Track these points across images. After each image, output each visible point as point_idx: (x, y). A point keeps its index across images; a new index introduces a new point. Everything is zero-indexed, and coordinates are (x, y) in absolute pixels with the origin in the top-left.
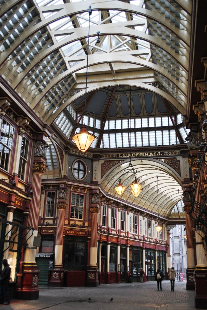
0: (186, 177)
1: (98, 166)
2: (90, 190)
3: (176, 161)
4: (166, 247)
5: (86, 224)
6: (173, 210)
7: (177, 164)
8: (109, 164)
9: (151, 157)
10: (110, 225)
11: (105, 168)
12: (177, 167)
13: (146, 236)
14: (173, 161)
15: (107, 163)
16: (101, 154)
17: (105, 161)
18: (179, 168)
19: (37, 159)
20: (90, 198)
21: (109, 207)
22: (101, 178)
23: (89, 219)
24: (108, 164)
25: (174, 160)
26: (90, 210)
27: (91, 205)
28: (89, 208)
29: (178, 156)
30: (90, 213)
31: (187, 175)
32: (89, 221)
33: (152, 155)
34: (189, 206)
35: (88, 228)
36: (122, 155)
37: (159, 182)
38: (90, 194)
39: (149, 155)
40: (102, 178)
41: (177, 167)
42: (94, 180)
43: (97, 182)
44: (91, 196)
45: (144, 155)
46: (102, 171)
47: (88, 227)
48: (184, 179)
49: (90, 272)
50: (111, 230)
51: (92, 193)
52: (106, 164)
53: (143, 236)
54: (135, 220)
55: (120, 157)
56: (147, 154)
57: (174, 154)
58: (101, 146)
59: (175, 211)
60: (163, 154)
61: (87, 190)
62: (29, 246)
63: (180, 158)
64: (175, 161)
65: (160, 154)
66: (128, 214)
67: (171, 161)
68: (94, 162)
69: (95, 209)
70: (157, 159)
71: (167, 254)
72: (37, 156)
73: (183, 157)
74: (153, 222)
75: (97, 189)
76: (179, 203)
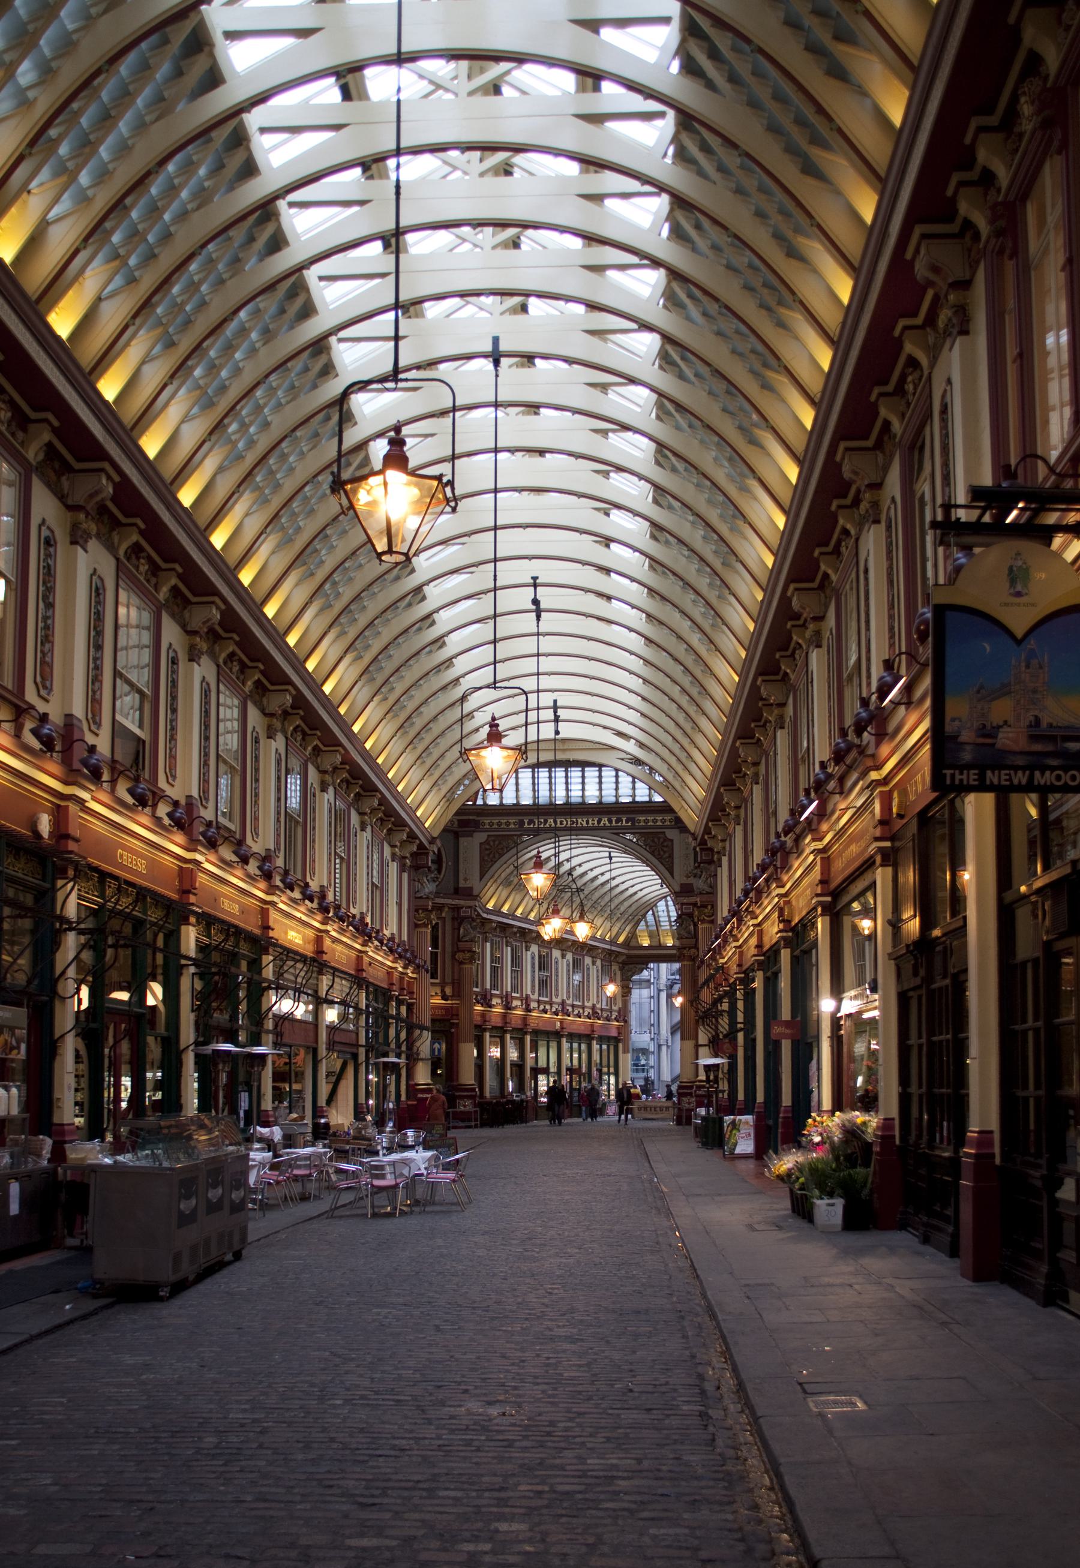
1: (471, 846)
2: (456, 909)
3: (665, 840)
4: (618, 1028)
5: (448, 991)
6: (643, 923)
9: (605, 828)
10: (488, 986)
12: (667, 855)
13: (569, 1002)
15: (494, 841)
18: (671, 856)
19: (421, 902)
20: (454, 929)
21: (486, 940)
23: (453, 979)
25: (659, 839)
29: (667, 827)
30: (456, 964)
32: (453, 983)
33: (608, 824)
36: (531, 822)
37: (614, 873)
38: (453, 919)
39: (599, 822)
42: (462, 884)
43: (471, 889)
45: (587, 822)
47: (453, 997)
48: (682, 885)
49: (462, 1097)
50: (492, 995)
51: (458, 918)
53: (563, 1003)
54: (544, 963)
55: (526, 826)
56: (593, 821)
57: (659, 823)
58: (480, 802)
59: (647, 926)
60: (633, 820)
61: (446, 909)
62: (422, 1056)
63: (671, 834)
65: (627, 822)
66: (527, 949)
67: (653, 841)
68: (461, 840)
69: (468, 955)
70: (618, 834)
71: (620, 1045)
72: (421, 898)
74: (588, 960)
75: (470, 907)
76: (661, 905)
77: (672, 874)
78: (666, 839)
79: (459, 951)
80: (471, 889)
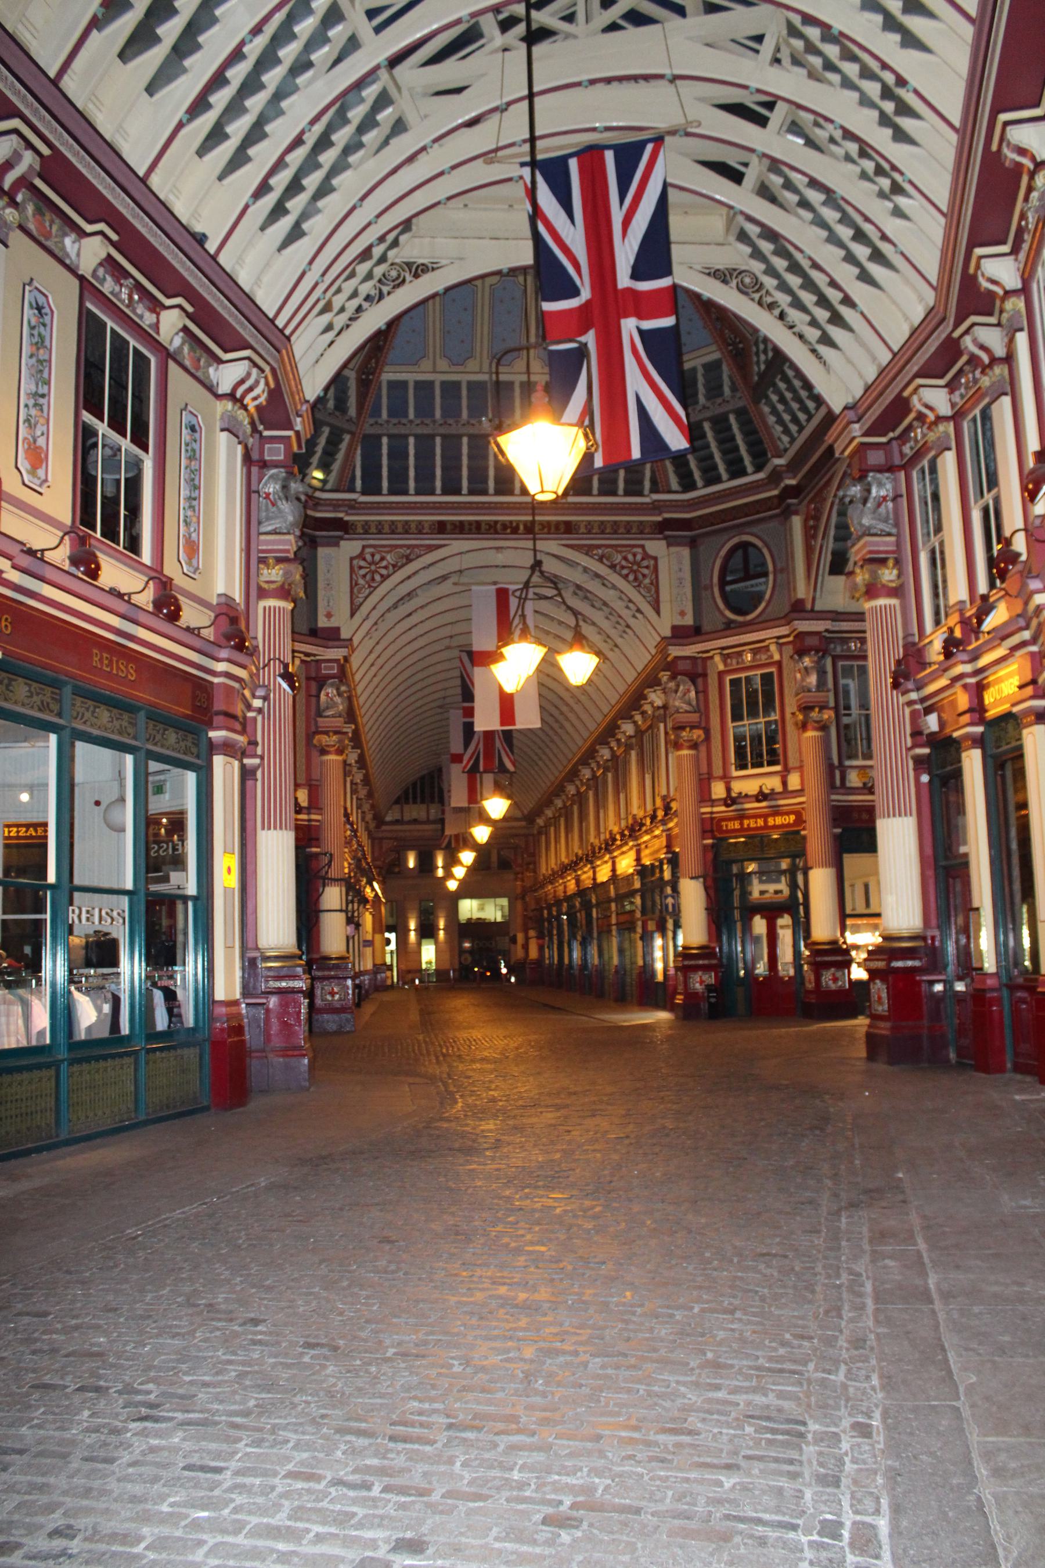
0: (679, 621)
7: (647, 567)
8: (382, 559)
11: (364, 576)
12: (647, 581)
14: (630, 557)
15: (373, 555)
16: (347, 518)
17: (364, 547)
18: (656, 584)
20: (309, 696)
22: (352, 615)
24: (377, 557)
25: (635, 555)
26: (315, 742)
27: (316, 722)
28: (309, 737)
30: (315, 753)
31: (682, 614)
34: (692, 728)
35: (309, 814)
38: (308, 679)
40: (352, 615)
41: (647, 581)
42: (322, 622)
43: (337, 630)
44: (314, 685)
46: (353, 585)
47: (309, 810)
52: (369, 557)
64: (639, 557)
67: (625, 558)
68: (322, 552)
73: (669, 545)
77: (658, 612)
78: (646, 556)
79: (317, 732)
80: (337, 630)
